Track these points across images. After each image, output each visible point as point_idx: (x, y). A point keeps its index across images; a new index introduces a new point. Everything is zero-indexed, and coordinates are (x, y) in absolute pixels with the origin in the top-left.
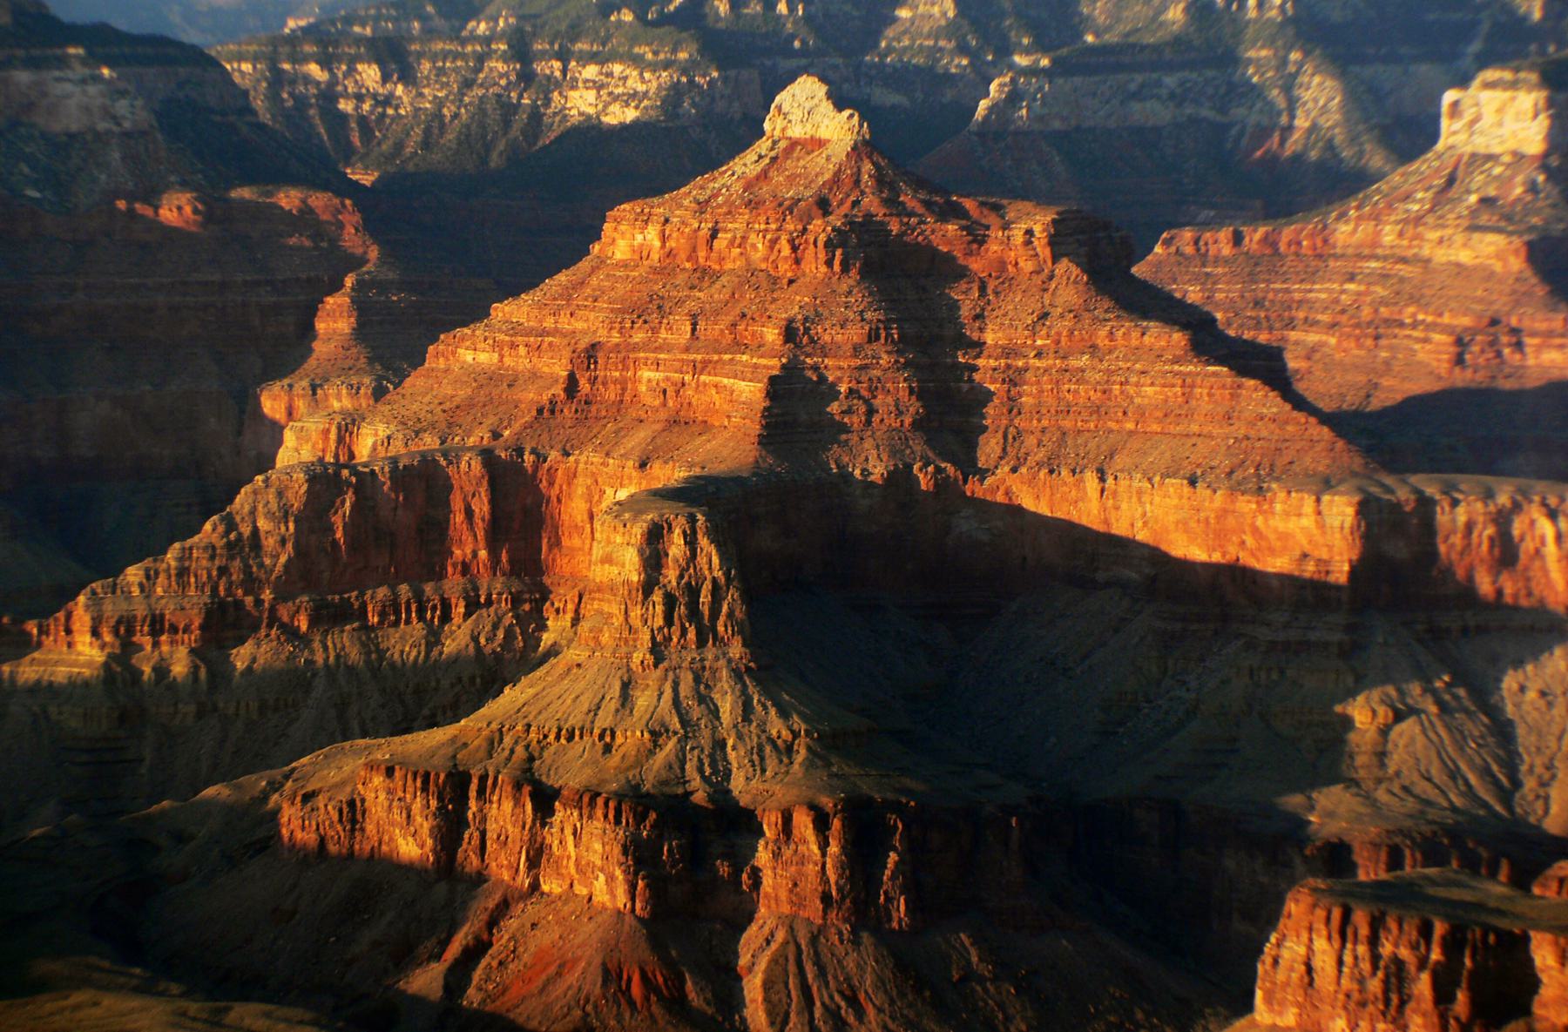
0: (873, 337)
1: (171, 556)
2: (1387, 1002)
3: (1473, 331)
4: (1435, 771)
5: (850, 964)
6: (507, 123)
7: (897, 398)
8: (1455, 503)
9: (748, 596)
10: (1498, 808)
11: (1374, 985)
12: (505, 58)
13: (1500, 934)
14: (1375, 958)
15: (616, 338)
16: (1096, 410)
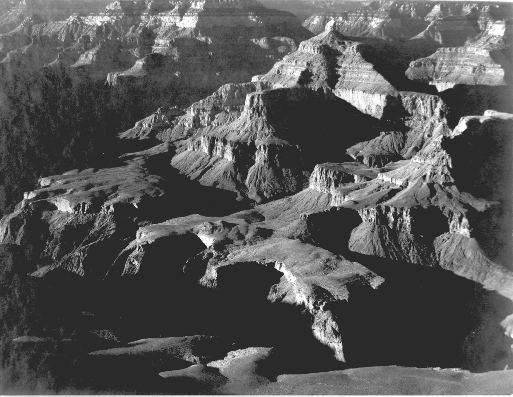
0: (322, 65)
1: (207, 99)
2: (327, 186)
3: (477, 67)
4: (389, 145)
5: (266, 173)
6: (361, 27)
7: (324, 75)
8: (405, 97)
9: (267, 109)
10: (397, 151)
11: (325, 183)
12: (363, 16)
13: (347, 175)
14: (326, 177)
15: (286, 64)
16: (356, 78)
